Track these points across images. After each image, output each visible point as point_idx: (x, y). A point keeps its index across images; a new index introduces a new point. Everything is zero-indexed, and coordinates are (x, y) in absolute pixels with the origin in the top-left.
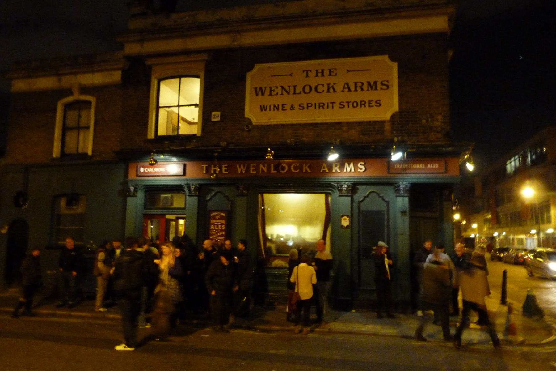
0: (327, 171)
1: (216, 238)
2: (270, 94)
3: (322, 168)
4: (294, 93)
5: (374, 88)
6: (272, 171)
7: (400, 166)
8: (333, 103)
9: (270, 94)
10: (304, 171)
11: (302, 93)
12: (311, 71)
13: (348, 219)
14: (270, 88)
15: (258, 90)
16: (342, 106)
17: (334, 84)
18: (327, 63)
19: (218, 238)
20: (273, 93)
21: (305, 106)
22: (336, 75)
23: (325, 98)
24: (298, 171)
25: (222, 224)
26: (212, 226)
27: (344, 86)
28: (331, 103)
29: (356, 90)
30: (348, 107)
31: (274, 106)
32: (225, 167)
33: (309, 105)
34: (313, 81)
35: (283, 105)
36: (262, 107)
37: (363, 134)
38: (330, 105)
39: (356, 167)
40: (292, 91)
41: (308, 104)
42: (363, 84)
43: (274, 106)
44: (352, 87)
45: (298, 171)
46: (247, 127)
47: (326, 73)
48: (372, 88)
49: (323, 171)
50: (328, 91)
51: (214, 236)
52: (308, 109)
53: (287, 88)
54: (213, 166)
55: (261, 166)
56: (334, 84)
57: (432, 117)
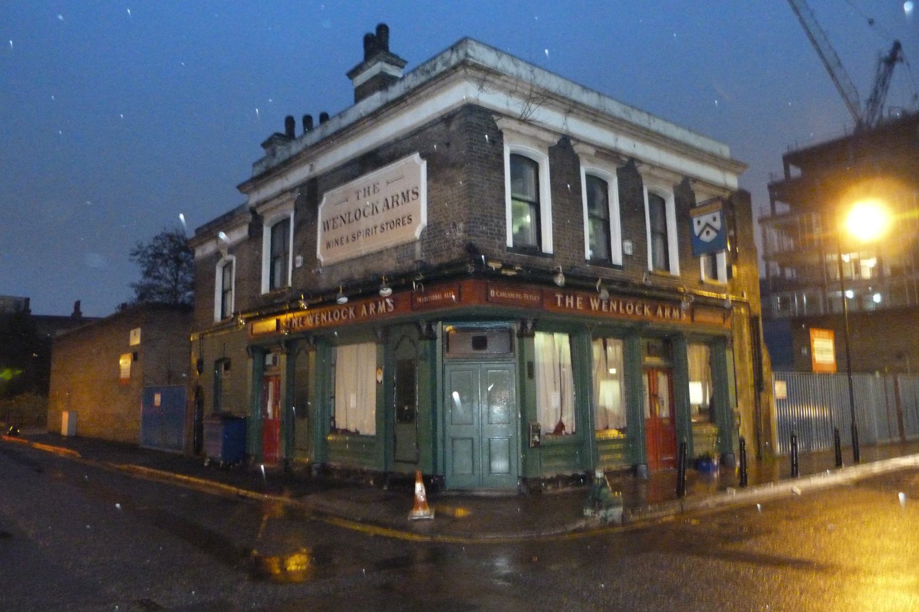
9: (334, 228)
11: (355, 219)
22: (379, 191)
37: (399, 262)
38: (374, 230)
42: (398, 196)
57: (455, 226)
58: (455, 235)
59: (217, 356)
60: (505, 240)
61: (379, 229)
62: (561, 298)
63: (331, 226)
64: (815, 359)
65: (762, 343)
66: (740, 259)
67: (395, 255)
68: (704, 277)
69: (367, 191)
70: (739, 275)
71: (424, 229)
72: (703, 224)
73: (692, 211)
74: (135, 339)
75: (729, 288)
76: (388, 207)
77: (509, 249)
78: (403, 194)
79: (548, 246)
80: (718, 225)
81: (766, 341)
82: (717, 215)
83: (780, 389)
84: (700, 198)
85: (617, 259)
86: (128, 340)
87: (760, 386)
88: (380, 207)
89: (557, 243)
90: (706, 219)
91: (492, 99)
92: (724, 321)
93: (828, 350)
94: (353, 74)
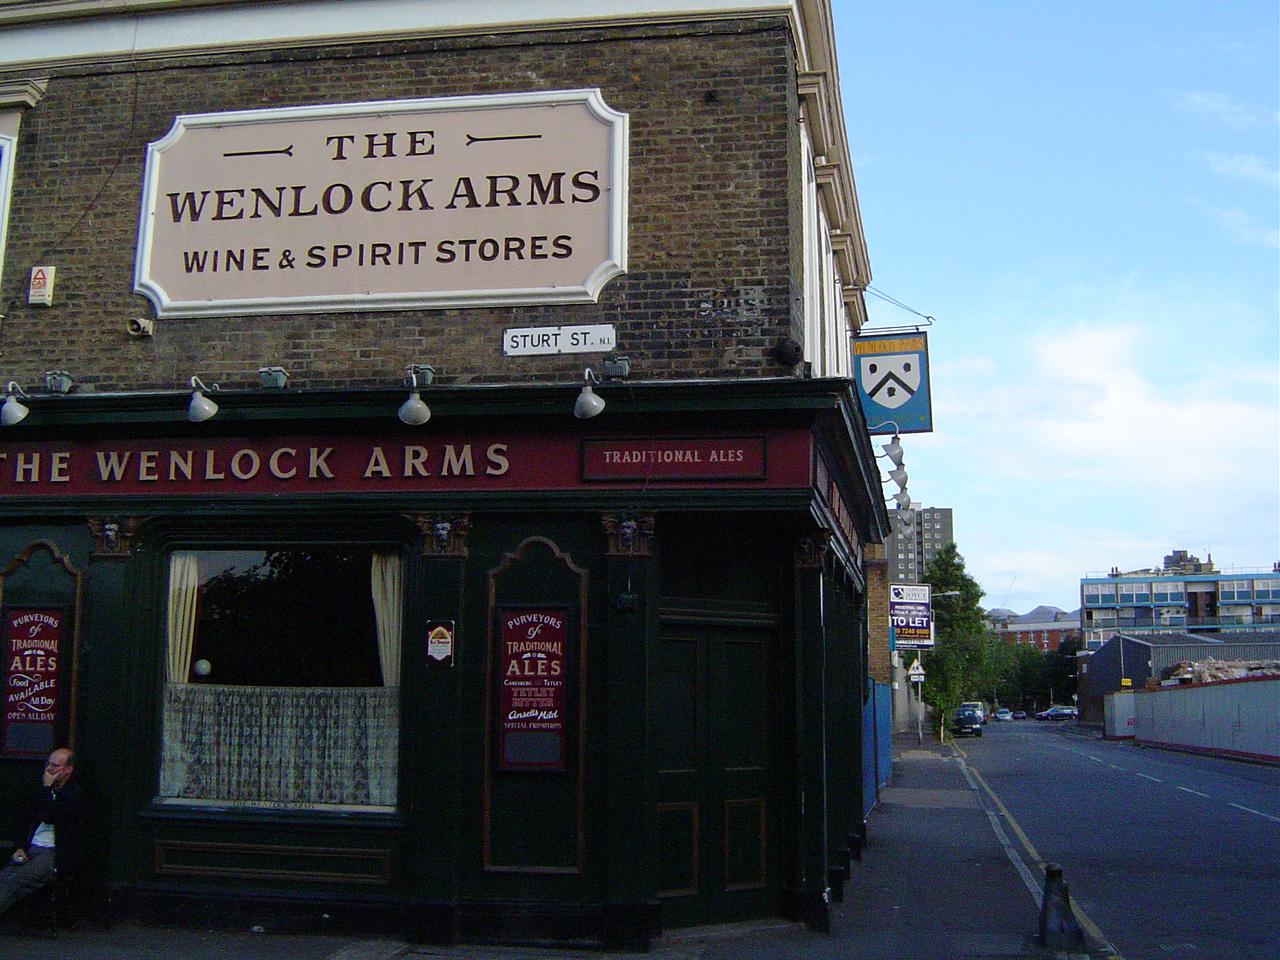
0: (386, 473)
1: (28, 699)
2: (219, 217)
3: (372, 461)
4: (296, 213)
5: (551, 196)
6: (210, 475)
7: (621, 458)
8: (417, 245)
9: (219, 217)
10: (313, 474)
11: (321, 208)
12: (352, 138)
13: (448, 635)
14: (221, 193)
15: (180, 200)
16: (446, 255)
17: (425, 181)
18: (401, 112)
19: (36, 701)
20: (227, 211)
22: (431, 152)
23: (394, 227)
24: (293, 472)
25: (48, 653)
26: (17, 658)
27: (456, 190)
28: (411, 244)
29: (493, 203)
30: (467, 259)
31: (230, 253)
32: (62, 460)
33: (342, 252)
34: (357, 172)
35: (256, 251)
36: (190, 256)
38: (409, 252)
39: (481, 461)
40: (288, 206)
41: (336, 247)
42: (516, 181)
43: (230, 253)
44: (482, 194)
45: (293, 472)
46: (135, 326)
47: (401, 144)
48: (544, 194)
49: (373, 472)
50: (406, 207)
51: (22, 696)
52: (335, 264)
54: (21, 457)
55: (175, 457)
56: (425, 181)
57: (731, 293)
58: (734, 312)
61: (429, 253)
69: (382, 145)
78: (536, 178)
82: (914, 360)
88: (439, 195)
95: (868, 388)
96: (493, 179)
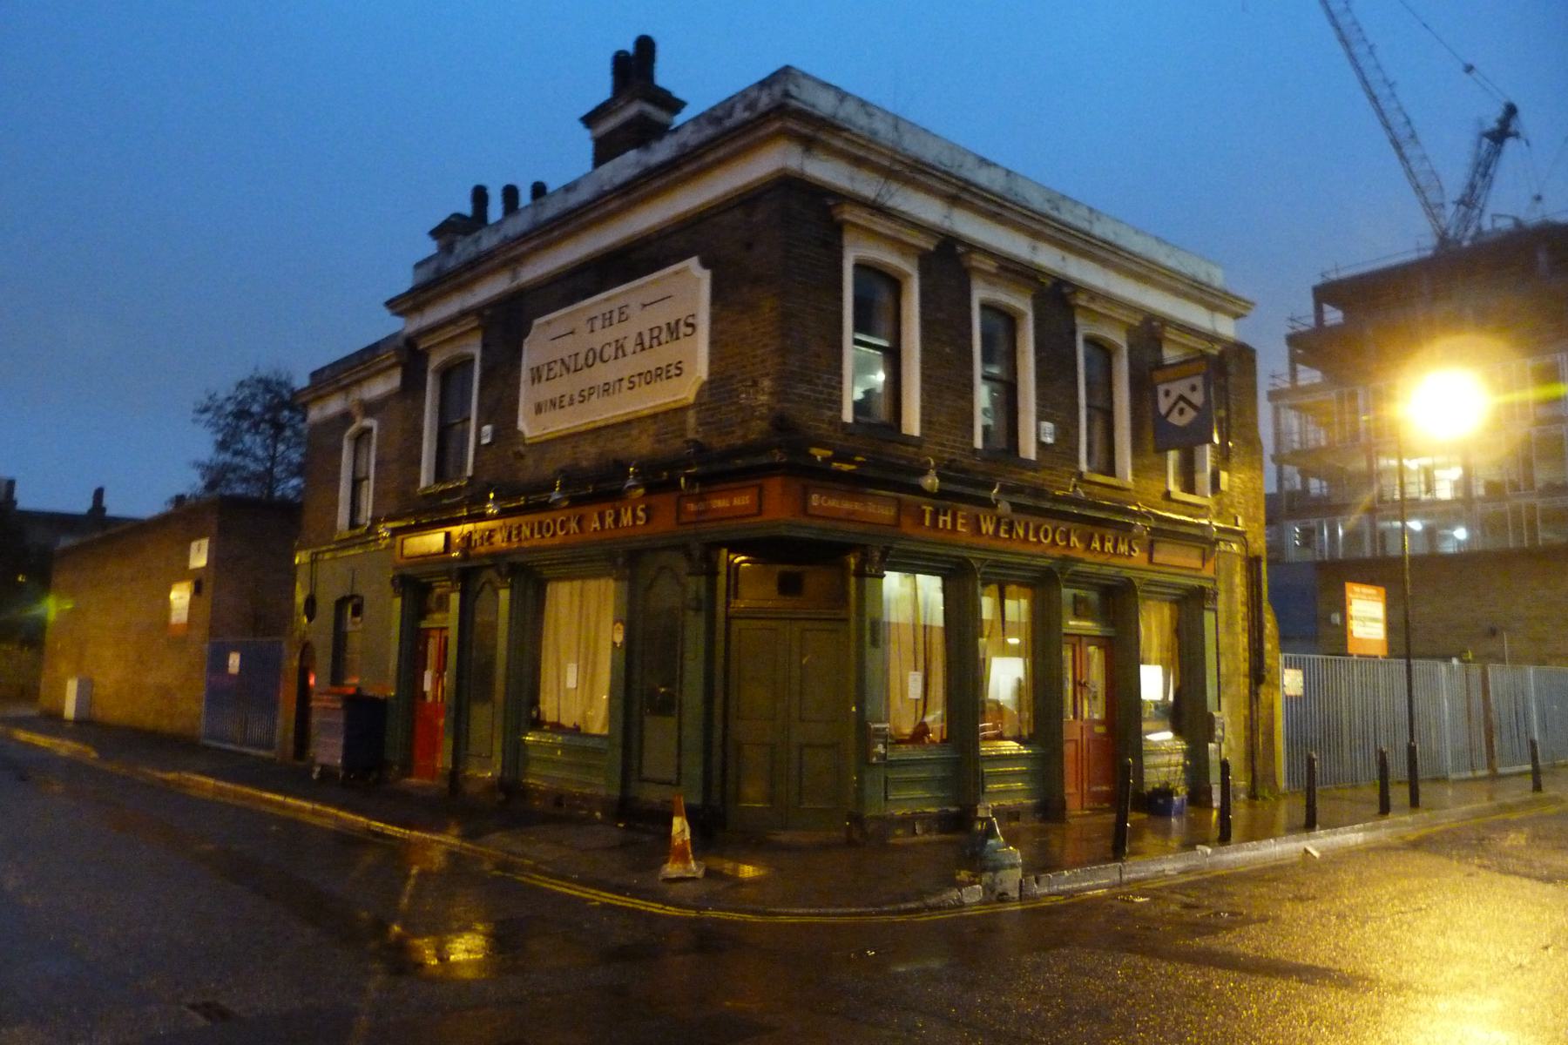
2: (548, 379)
13: (621, 627)
21: (586, 393)
29: (651, 347)
40: (572, 368)
44: (647, 344)
50: (616, 358)
53: (567, 359)
57: (755, 383)
59: (339, 594)
60: (840, 410)
61: (625, 384)
62: (931, 512)
63: (544, 378)
64: (1352, 632)
65: (1265, 604)
66: (1234, 460)
67: (652, 429)
68: (1173, 487)
70: (1231, 488)
71: (704, 383)
72: (1174, 396)
73: (1158, 375)
74: (199, 558)
75: (1214, 509)
76: (642, 344)
77: (846, 425)
79: (912, 424)
80: (1198, 398)
81: (1272, 600)
82: (1198, 381)
83: (1292, 681)
84: (1170, 355)
85: (1029, 450)
86: (187, 558)
87: (1258, 674)
88: (630, 346)
89: (926, 421)
90: (1179, 388)
91: (825, 171)
92: (1203, 565)
93: (1374, 620)
94: (590, 120)
95: (1163, 408)
96: (651, 330)
